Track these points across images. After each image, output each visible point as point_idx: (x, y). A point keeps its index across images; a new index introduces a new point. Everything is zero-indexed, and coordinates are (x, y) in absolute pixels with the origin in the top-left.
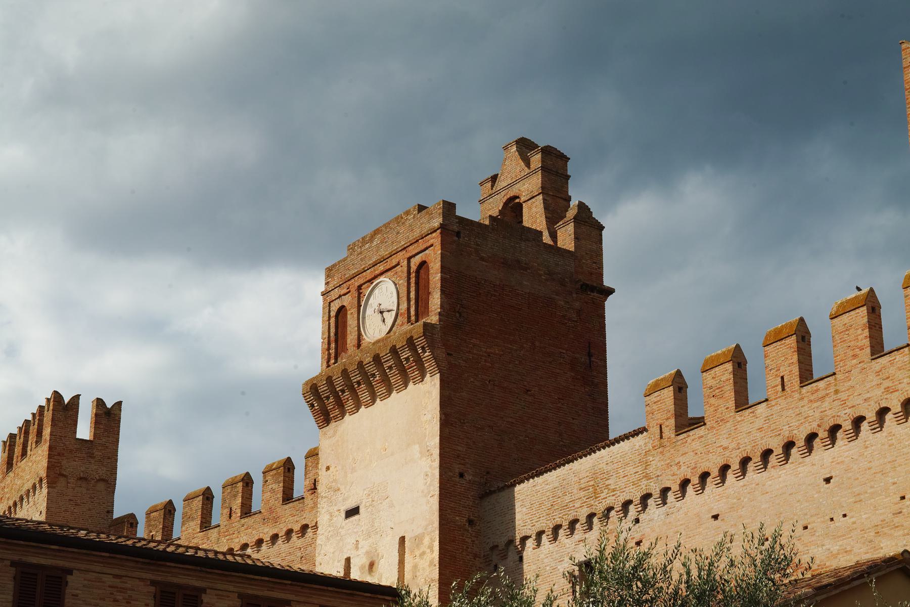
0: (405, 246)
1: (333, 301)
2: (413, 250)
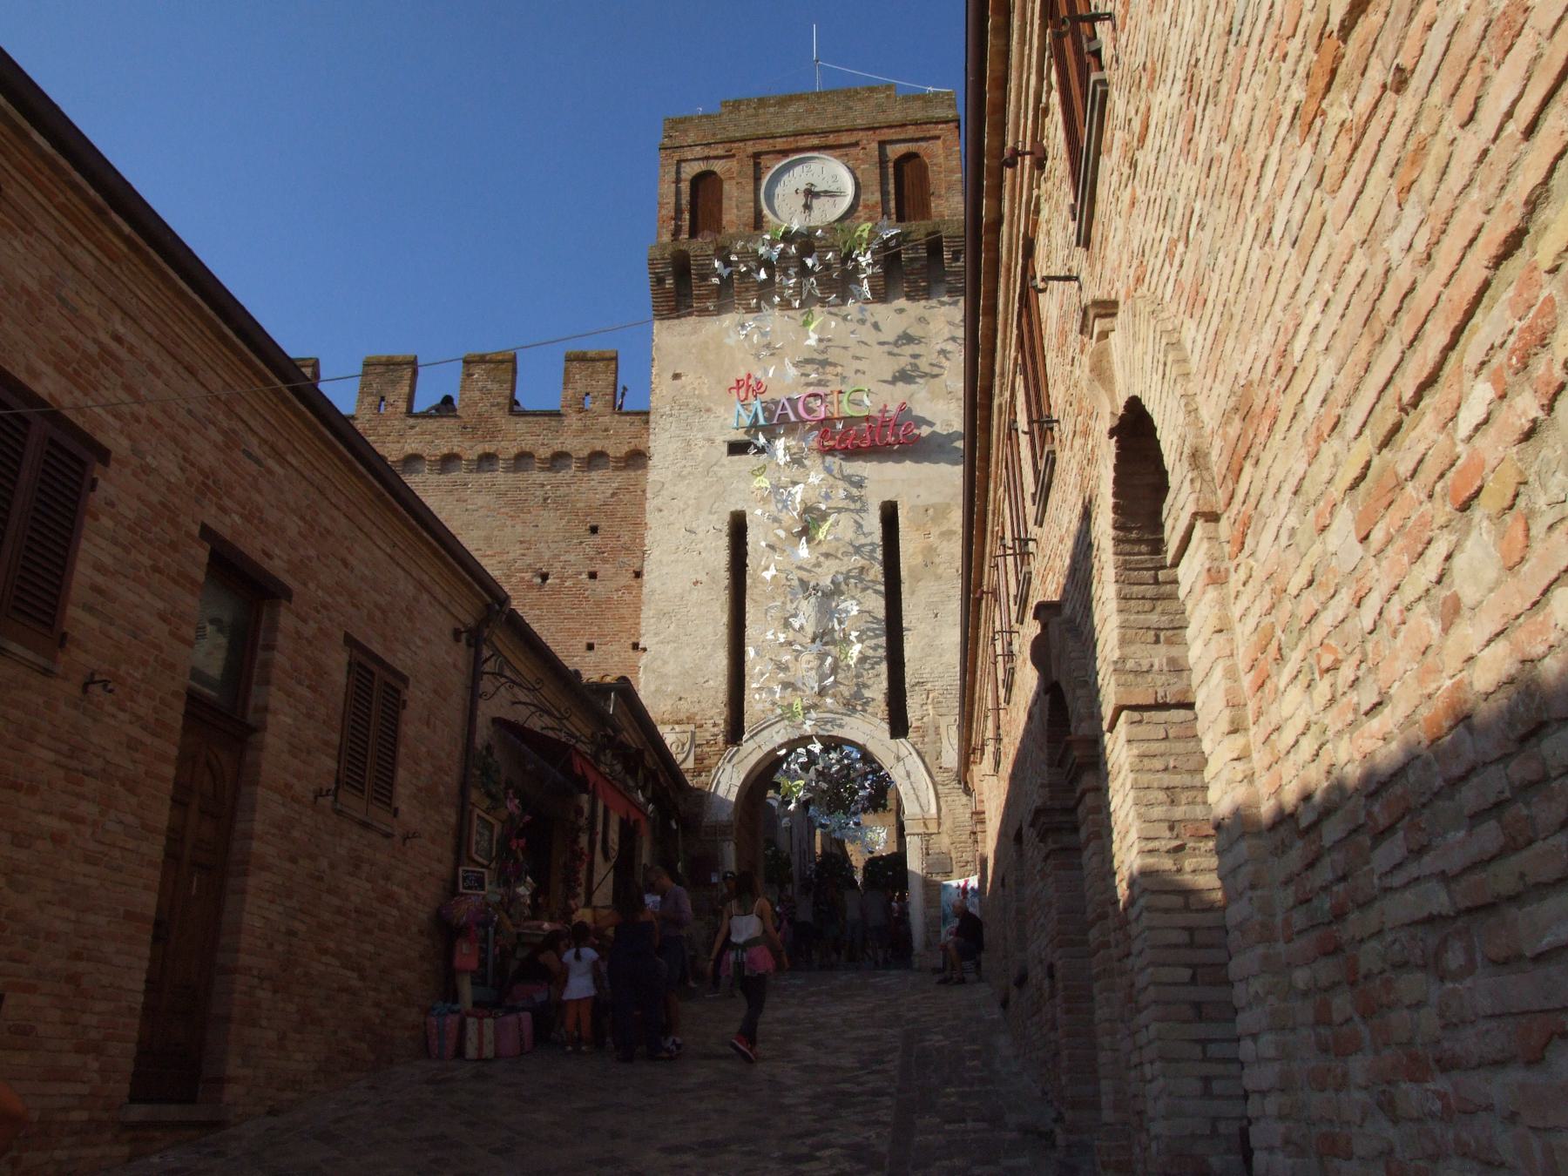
1: (687, 160)
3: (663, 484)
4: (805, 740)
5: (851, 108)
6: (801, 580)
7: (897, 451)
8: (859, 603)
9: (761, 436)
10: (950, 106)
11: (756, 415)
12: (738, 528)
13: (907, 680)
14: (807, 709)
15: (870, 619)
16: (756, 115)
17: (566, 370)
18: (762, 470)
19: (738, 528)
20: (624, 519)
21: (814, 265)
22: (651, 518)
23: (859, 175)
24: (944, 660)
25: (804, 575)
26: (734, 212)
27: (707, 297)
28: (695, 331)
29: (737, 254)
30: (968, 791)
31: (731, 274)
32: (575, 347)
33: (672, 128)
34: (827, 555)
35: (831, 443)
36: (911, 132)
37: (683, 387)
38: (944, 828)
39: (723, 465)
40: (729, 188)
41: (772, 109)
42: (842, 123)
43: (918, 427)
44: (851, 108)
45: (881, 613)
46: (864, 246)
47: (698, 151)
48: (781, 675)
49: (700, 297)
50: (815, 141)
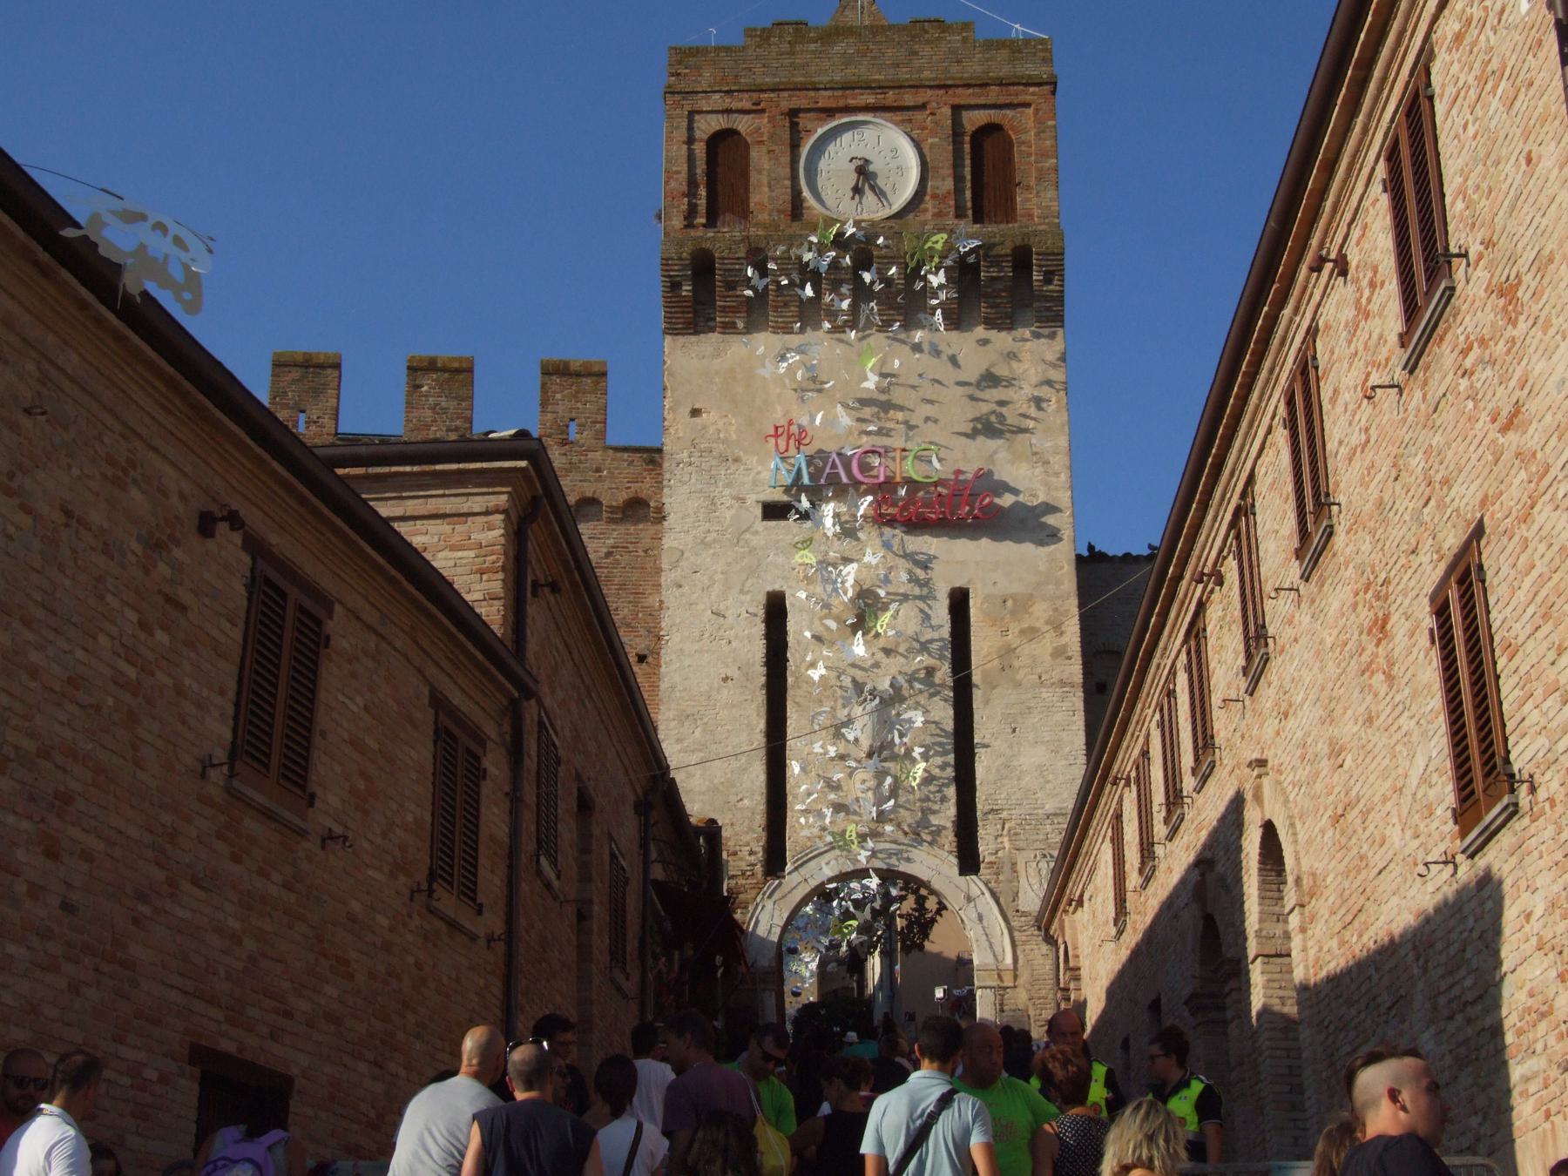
0: (950, 82)
2: (965, 96)
3: (683, 554)
4: (862, 874)
5: (915, 53)
6: (854, 680)
7: (970, 525)
8: (926, 712)
9: (804, 498)
10: (1044, 60)
11: (799, 470)
12: (776, 611)
13: (979, 806)
14: (862, 838)
15: (938, 731)
16: (792, 53)
17: (543, 385)
18: (807, 543)
19: (776, 611)
20: (622, 586)
21: (873, 283)
22: (670, 596)
23: (926, 151)
24: (1023, 783)
25: (859, 675)
26: (765, 194)
27: (734, 310)
28: (717, 354)
29: (775, 259)
30: (1050, 940)
31: (766, 287)
32: (556, 355)
33: (679, 63)
34: (887, 652)
35: (892, 511)
36: (994, 95)
37: (704, 427)
38: (1021, 981)
39: (756, 533)
40: (757, 156)
41: (812, 47)
42: (904, 74)
43: (999, 495)
44: (915, 53)
45: (949, 725)
46: (936, 260)
47: (717, 101)
48: (832, 796)
49: (724, 309)
50: (869, 99)
